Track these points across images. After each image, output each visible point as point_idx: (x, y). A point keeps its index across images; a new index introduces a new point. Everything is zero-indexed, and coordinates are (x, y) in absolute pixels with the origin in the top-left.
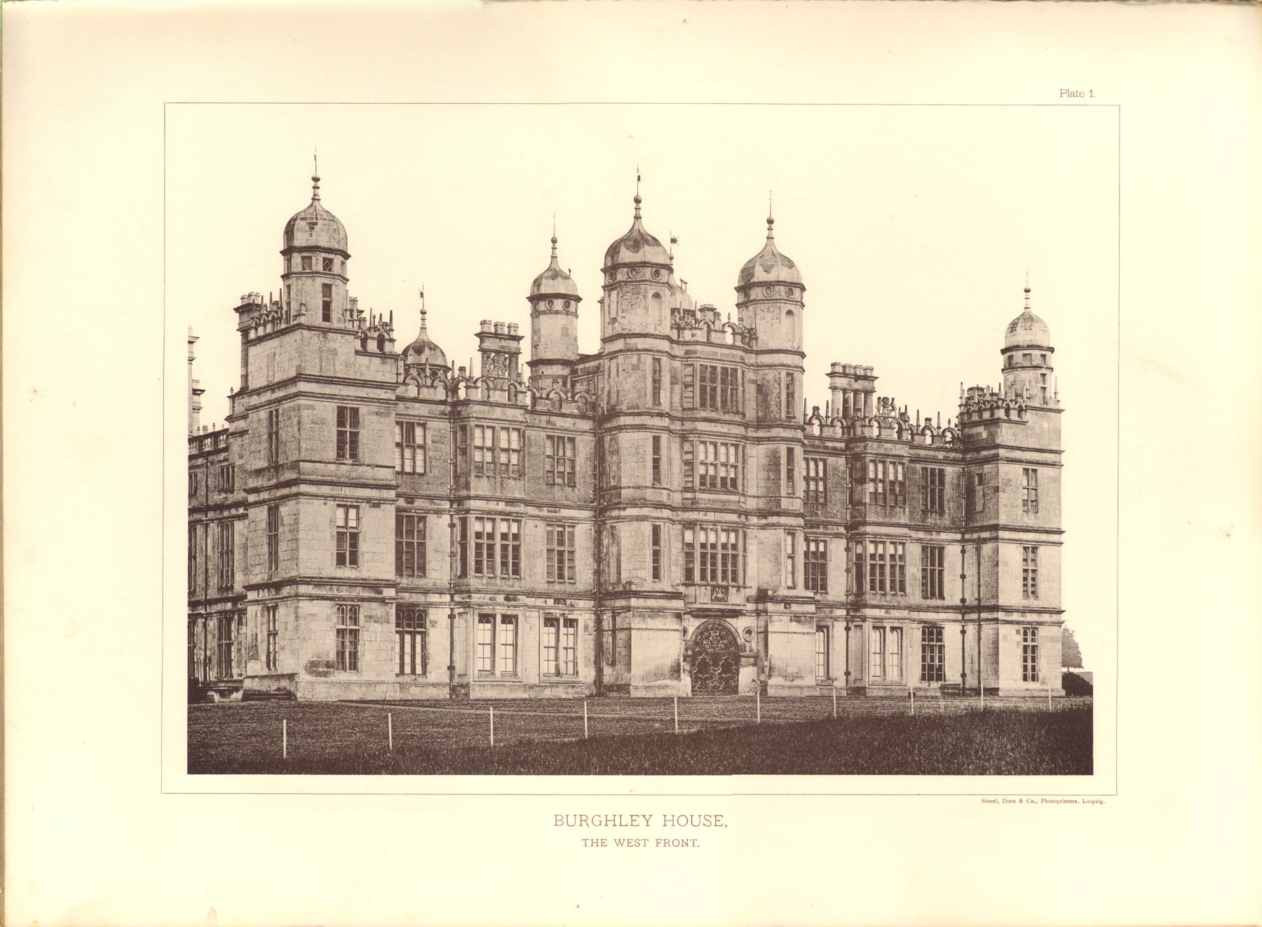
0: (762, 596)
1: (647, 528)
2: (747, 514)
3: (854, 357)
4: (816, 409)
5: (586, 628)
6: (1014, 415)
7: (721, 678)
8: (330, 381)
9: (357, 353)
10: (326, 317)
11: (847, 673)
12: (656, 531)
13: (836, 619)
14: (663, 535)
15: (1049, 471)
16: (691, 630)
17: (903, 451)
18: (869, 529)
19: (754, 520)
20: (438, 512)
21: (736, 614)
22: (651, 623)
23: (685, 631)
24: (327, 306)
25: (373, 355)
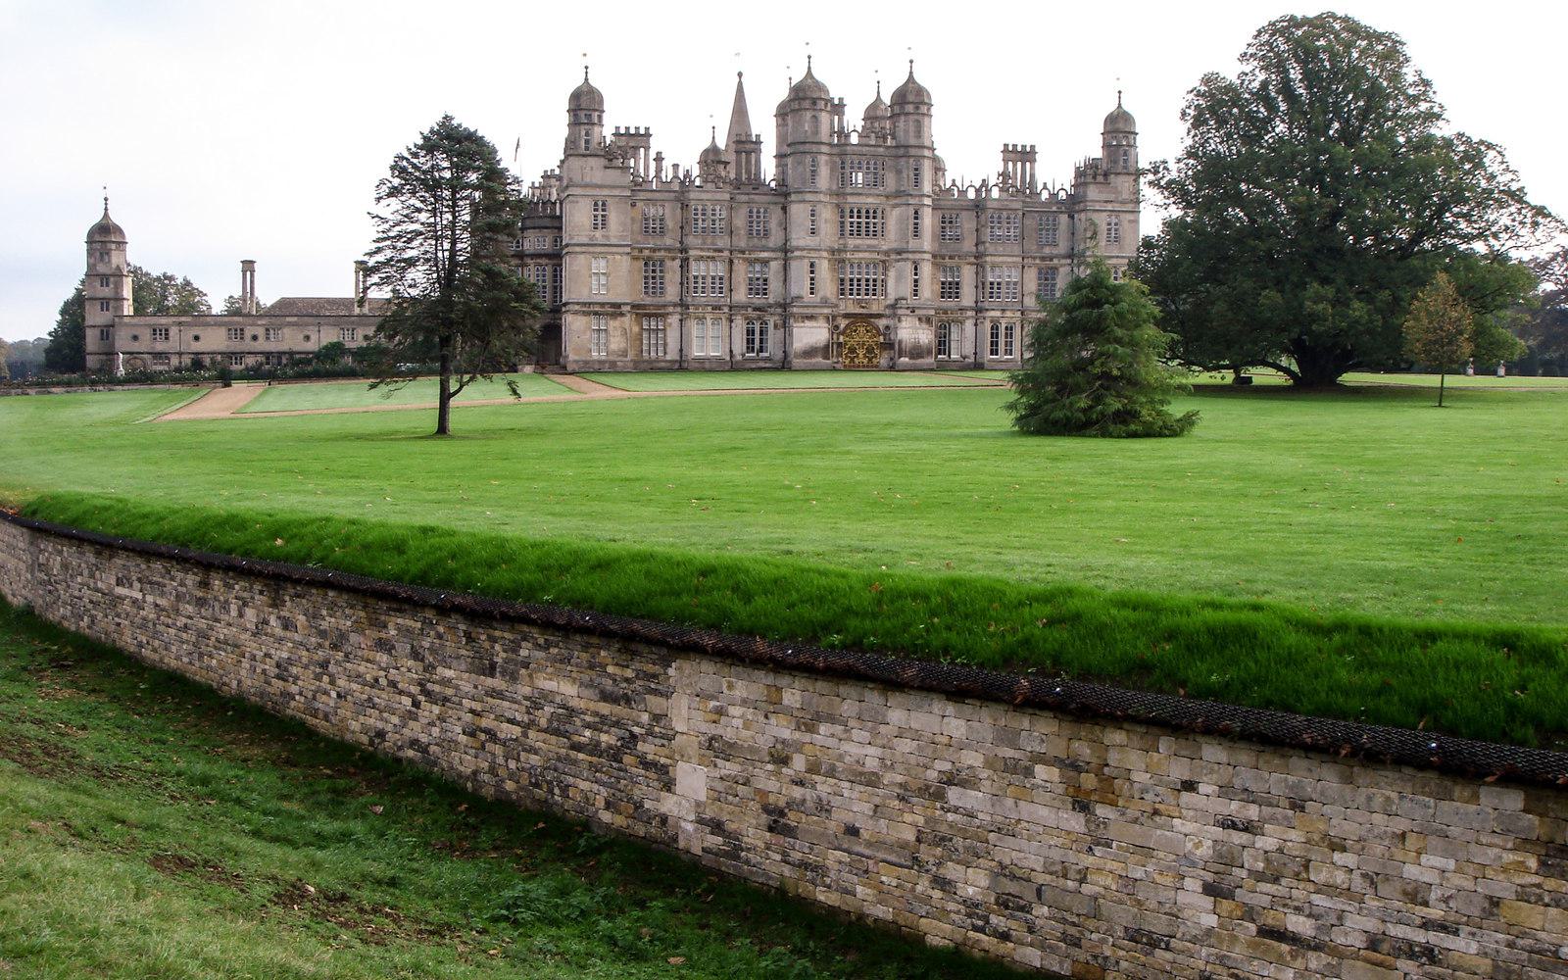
0: (893, 306)
1: (806, 263)
2: (887, 253)
3: (1021, 140)
4: (954, 181)
5: (776, 326)
6: (1100, 179)
7: (865, 356)
8: (586, 186)
9: (606, 167)
10: (587, 149)
11: (975, 354)
12: (812, 265)
13: (967, 318)
14: (817, 269)
15: (1130, 217)
16: (842, 326)
17: (1018, 205)
18: (988, 259)
19: (893, 257)
20: (674, 259)
21: (879, 316)
22: (808, 323)
23: (837, 327)
24: (587, 142)
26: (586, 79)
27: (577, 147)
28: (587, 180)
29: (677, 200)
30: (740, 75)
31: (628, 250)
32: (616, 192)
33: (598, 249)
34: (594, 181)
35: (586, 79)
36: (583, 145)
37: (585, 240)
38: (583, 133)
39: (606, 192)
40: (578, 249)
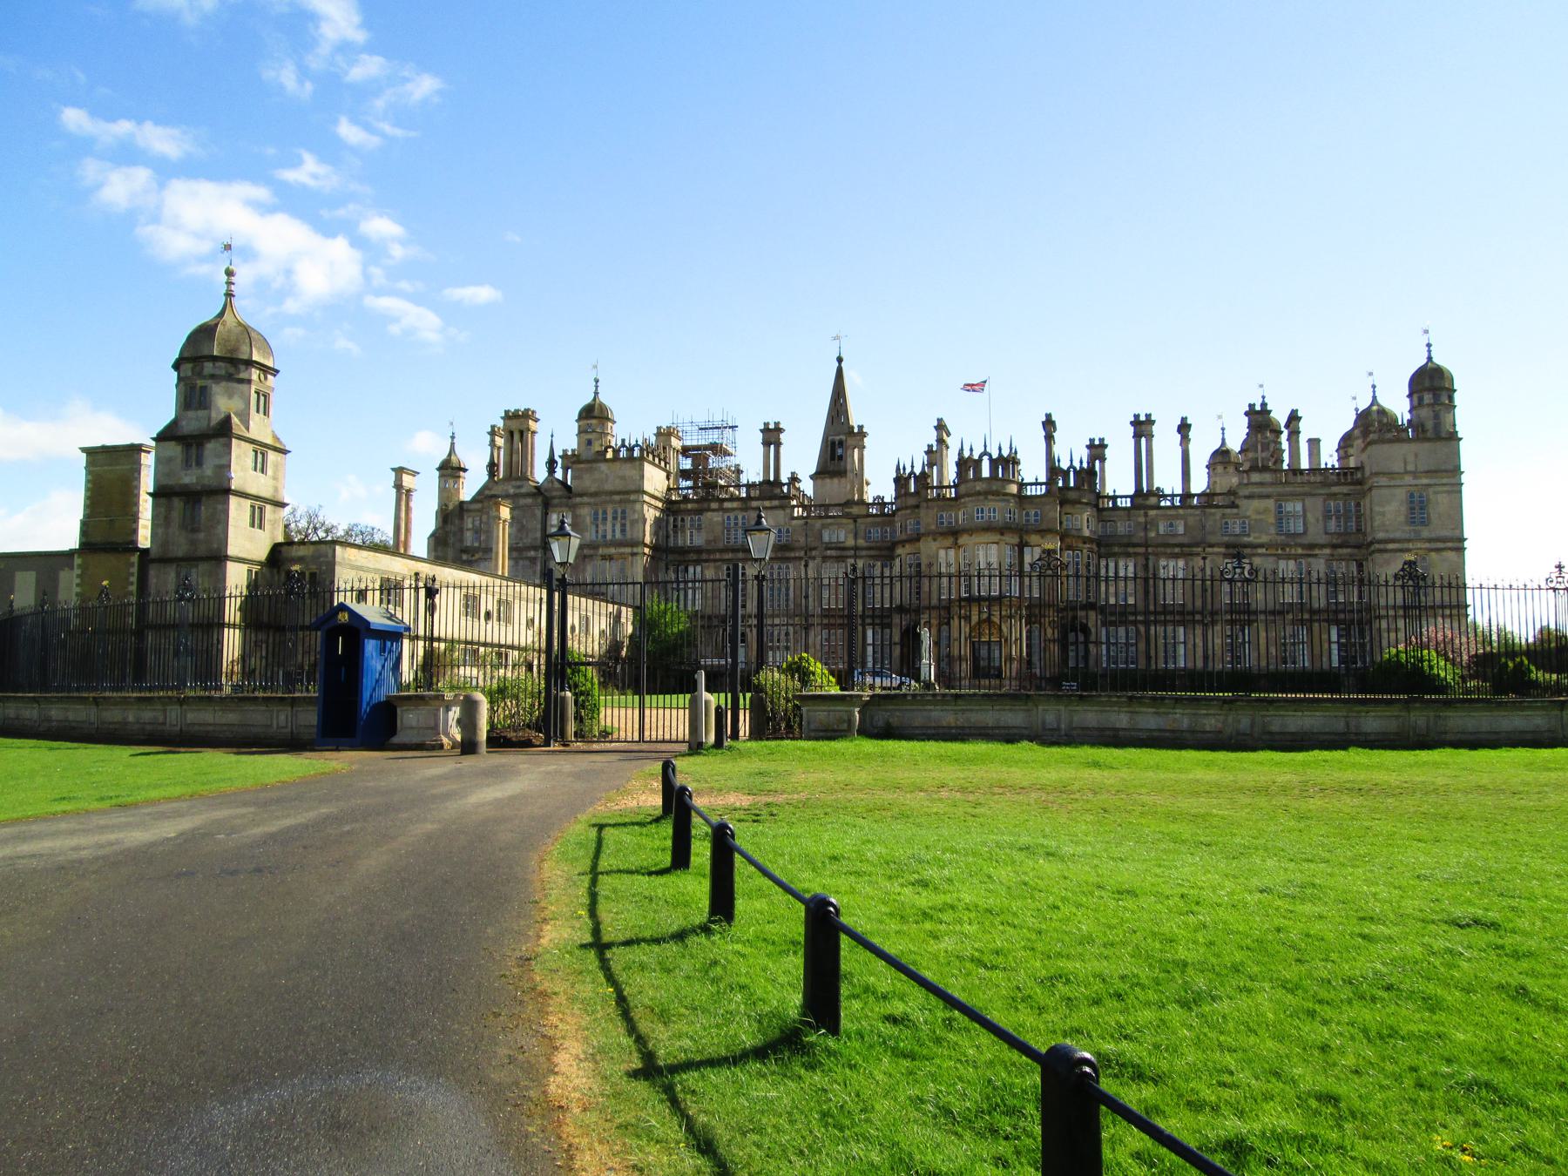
26: (1430, 358)
30: (840, 360)
35: (1430, 358)
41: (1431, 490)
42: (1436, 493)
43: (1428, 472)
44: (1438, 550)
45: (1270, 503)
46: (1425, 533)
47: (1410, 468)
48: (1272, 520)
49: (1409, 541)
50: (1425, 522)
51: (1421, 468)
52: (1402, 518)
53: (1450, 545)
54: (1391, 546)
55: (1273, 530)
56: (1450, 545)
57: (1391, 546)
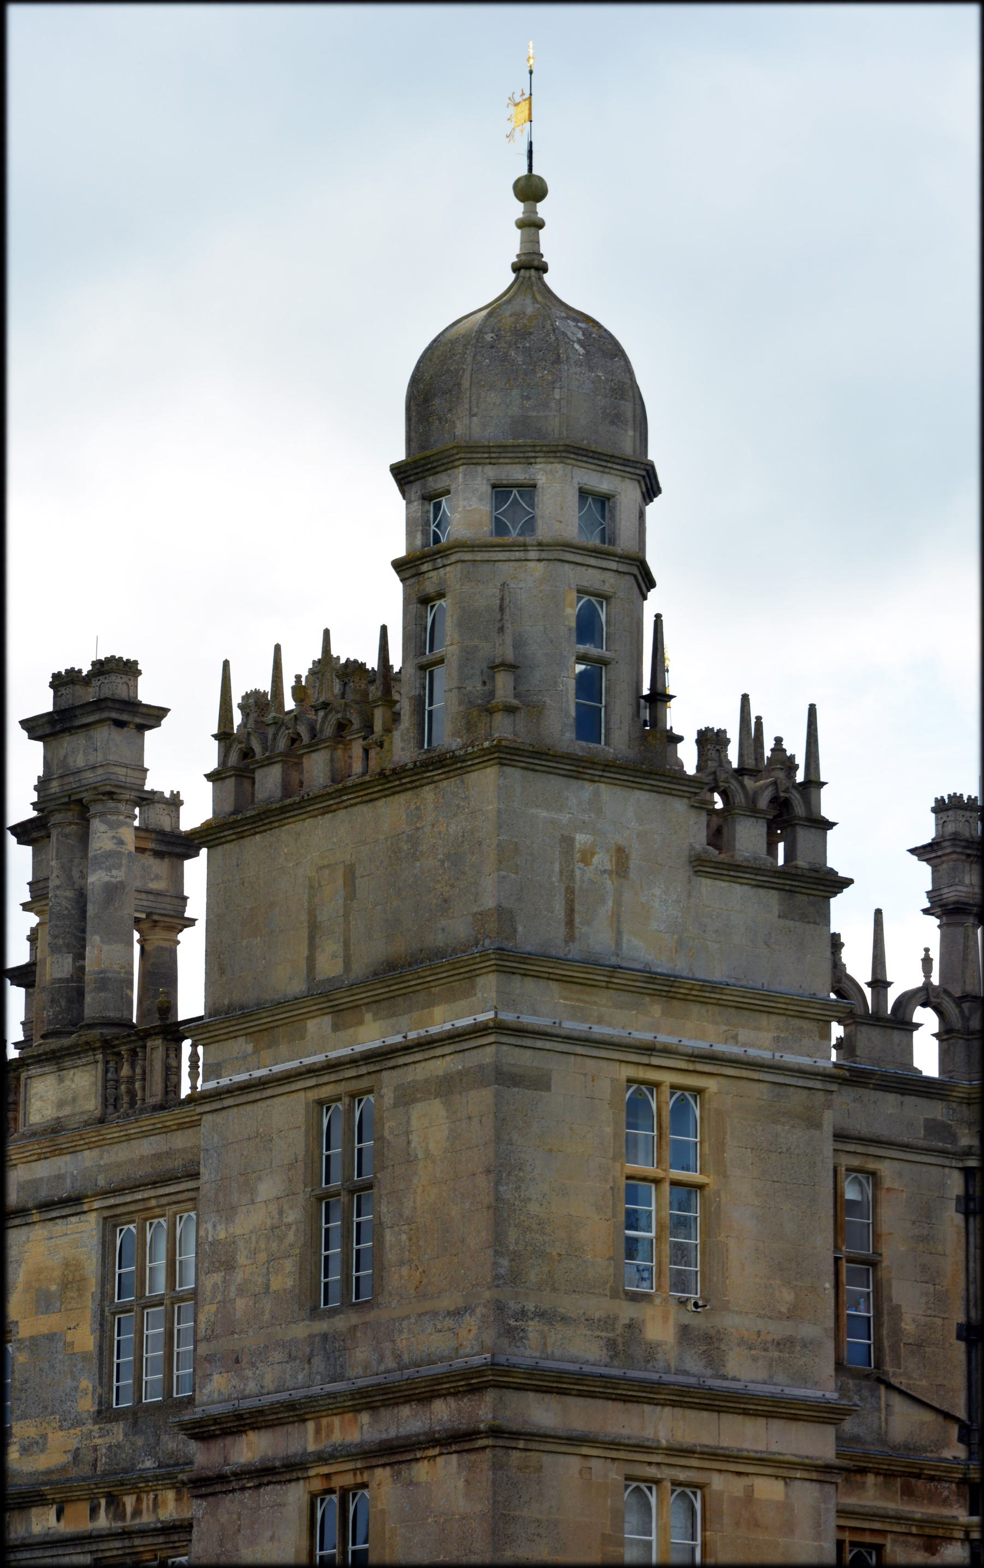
9: (701, 866)
10: (588, 723)
25: (734, 871)
26: (530, 266)
27: (524, 706)
28: (597, 937)
29: (936, 1142)
31: (818, 1444)
32: (758, 1040)
33: (664, 1425)
34: (646, 948)
35: (530, 266)
36: (562, 706)
37: (583, 1350)
38: (571, 612)
39: (699, 1031)
40: (543, 1413)
41: (390, 1081)
42: (406, 1098)
43: (399, 978)
44: (396, 1453)
45: (83, 1232)
46: (365, 1363)
47: (329, 966)
48: (85, 1338)
49: (291, 1412)
50: (358, 1295)
51: (359, 969)
52: (285, 1279)
53: (443, 1413)
54: (250, 1449)
55: (87, 1405)
56: (443, 1413)
57: (250, 1449)
